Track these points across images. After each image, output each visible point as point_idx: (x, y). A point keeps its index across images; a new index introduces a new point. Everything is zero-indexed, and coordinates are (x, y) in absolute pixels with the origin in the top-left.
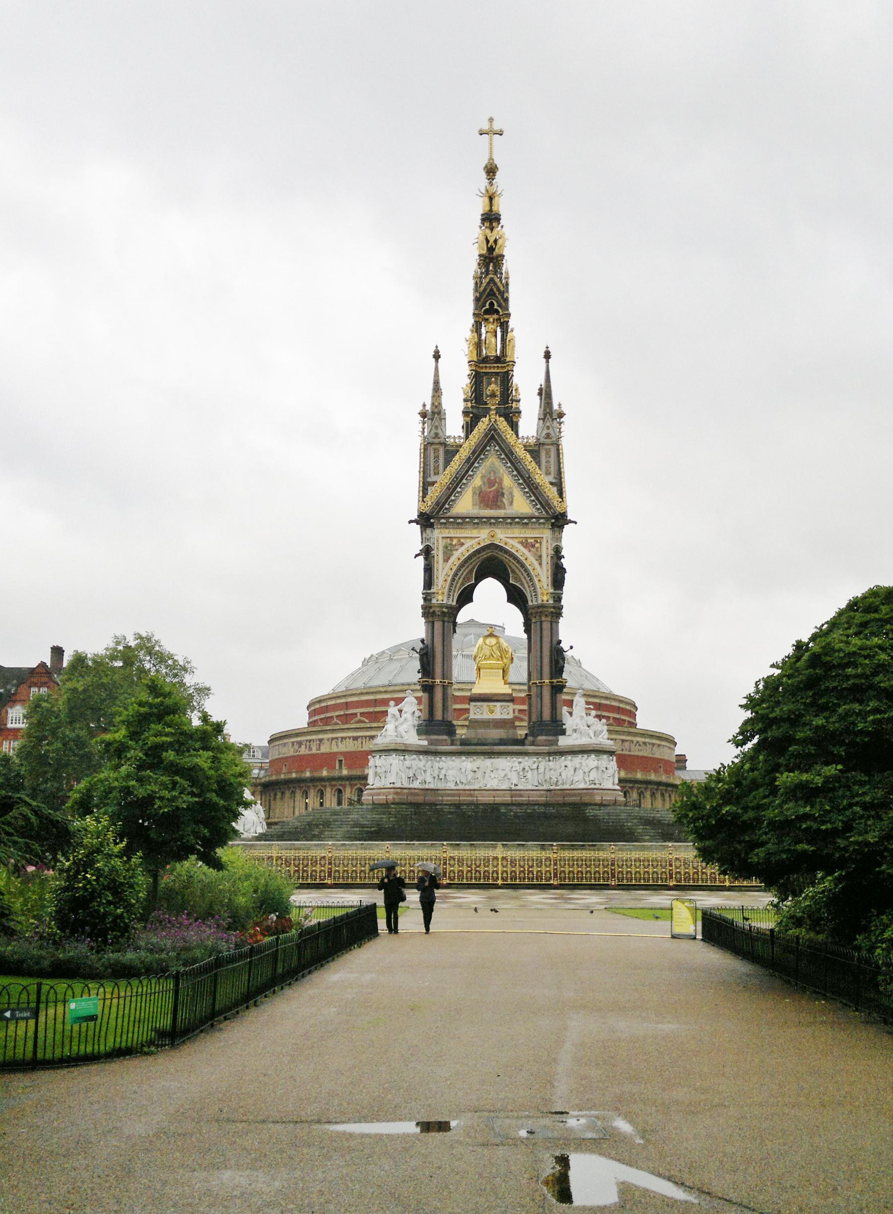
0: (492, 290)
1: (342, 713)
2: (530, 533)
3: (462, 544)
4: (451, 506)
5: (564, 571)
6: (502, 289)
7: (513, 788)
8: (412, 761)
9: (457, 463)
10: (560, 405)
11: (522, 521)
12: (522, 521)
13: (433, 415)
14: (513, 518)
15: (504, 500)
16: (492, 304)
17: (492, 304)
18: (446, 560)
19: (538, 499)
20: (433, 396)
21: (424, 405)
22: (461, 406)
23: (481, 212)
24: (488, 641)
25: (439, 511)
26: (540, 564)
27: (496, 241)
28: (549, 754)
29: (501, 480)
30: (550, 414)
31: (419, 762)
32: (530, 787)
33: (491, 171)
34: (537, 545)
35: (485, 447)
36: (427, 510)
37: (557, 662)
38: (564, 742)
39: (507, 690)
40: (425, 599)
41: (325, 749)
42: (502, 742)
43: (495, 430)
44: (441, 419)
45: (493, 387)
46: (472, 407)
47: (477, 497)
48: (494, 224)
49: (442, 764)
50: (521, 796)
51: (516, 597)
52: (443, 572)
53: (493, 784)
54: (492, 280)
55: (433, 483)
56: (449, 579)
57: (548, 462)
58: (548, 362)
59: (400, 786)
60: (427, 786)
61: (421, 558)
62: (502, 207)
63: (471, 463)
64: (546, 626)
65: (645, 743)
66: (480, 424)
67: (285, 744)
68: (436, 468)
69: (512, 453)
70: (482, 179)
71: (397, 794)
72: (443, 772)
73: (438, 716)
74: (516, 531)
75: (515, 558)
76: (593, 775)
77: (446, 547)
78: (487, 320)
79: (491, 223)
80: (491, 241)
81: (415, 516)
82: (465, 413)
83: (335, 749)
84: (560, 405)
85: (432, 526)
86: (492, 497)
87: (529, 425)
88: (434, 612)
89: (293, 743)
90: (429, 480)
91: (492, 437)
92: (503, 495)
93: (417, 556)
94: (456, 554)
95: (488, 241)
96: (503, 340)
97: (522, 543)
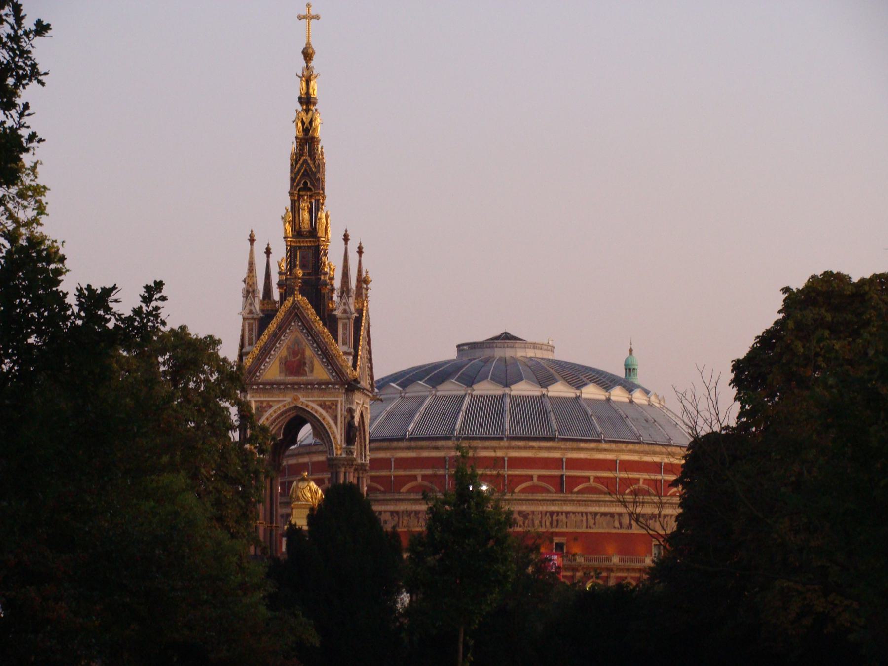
3: (271, 406)
10: (367, 272)
11: (322, 386)
12: (322, 386)
15: (307, 369)
16: (305, 183)
17: (305, 183)
27: (311, 122)
33: (308, 55)
34: (334, 407)
43: (298, 309)
46: (286, 279)
47: (283, 366)
54: (305, 161)
55: (247, 353)
80: (307, 122)
84: (367, 272)
86: (295, 365)
92: (305, 363)
97: (321, 405)
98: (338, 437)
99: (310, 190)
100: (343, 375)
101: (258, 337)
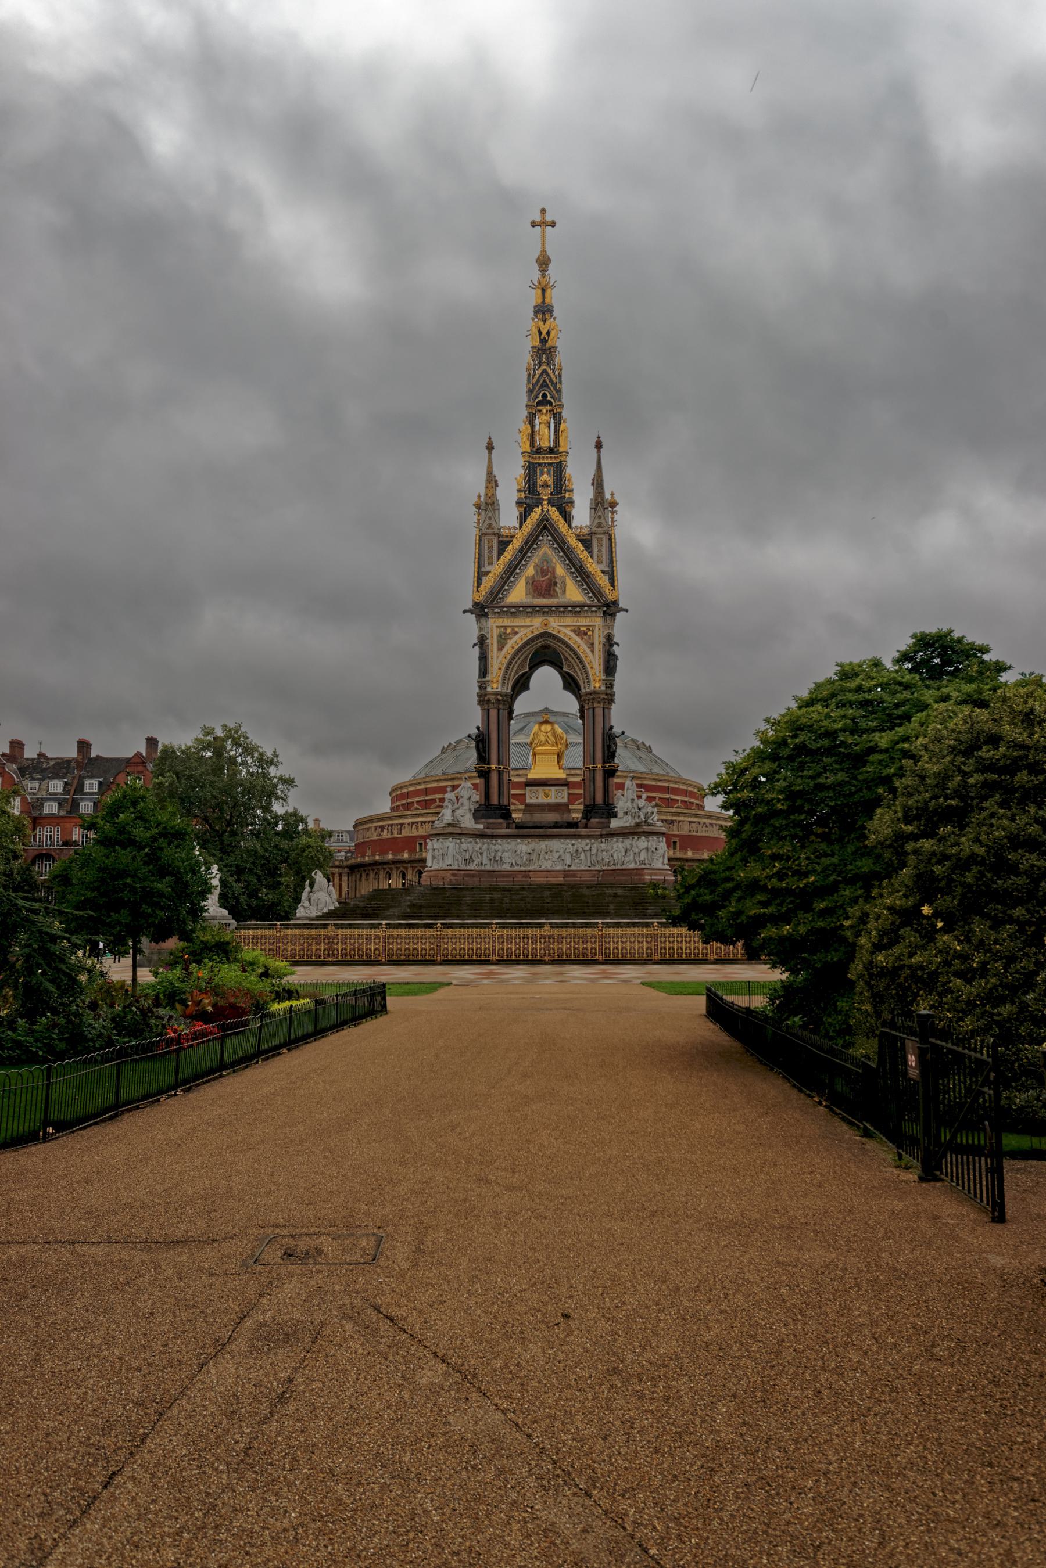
0: (545, 381)
1: (422, 798)
2: (582, 622)
3: (516, 633)
4: (505, 596)
5: (616, 658)
6: (554, 380)
7: (567, 868)
8: (467, 844)
9: (509, 553)
10: (612, 495)
13: (488, 506)
14: (566, 607)
15: (557, 590)
16: (545, 396)
17: (545, 396)
18: (500, 649)
19: (589, 587)
20: (487, 487)
21: (479, 497)
22: (515, 496)
23: (534, 304)
24: (543, 728)
25: (494, 600)
26: (593, 651)
27: (548, 333)
28: (601, 836)
29: (554, 569)
30: (602, 504)
31: (479, 845)
32: (583, 868)
33: (544, 262)
34: (590, 633)
35: (538, 536)
36: (480, 598)
37: (609, 747)
38: (614, 823)
39: (561, 775)
40: (480, 687)
41: (405, 833)
42: (556, 825)
43: (548, 520)
44: (494, 510)
45: (545, 477)
48: (547, 316)
49: (497, 847)
50: (574, 876)
51: (571, 684)
52: (498, 661)
53: (547, 865)
54: (545, 372)
55: (487, 573)
56: (504, 667)
57: (600, 551)
58: (599, 452)
59: (456, 867)
60: (483, 868)
61: (477, 647)
62: (554, 298)
63: (524, 553)
64: (599, 712)
65: (711, 825)
66: (533, 514)
67: (368, 829)
68: (490, 558)
69: (564, 543)
70: (535, 274)
71: (454, 875)
72: (499, 854)
73: (495, 800)
74: (568, 619)
75: (568, 646)
76: (643, 856)
77: (500, 636)
78: (540, 411)
79: (544, 314)
80: (544, 332)
81: (470, 606)
82: (519, 503)
83: (415, 833)
84: (612, 495)
85: (486, 615)
86: (544, 585)
87: (582, 515)
88: (489, 700)
89: (376, 828)
90: (483, 570)
91: (545, 526)
92: (555, 584)
93: (475, 645)
94: (510, 643)
95: (540, 333)
96: (556, 430)
97: (574, 631)
98: (596, 666)
99: (550, 403)
100: (602, 596)
101: (501, 553)
